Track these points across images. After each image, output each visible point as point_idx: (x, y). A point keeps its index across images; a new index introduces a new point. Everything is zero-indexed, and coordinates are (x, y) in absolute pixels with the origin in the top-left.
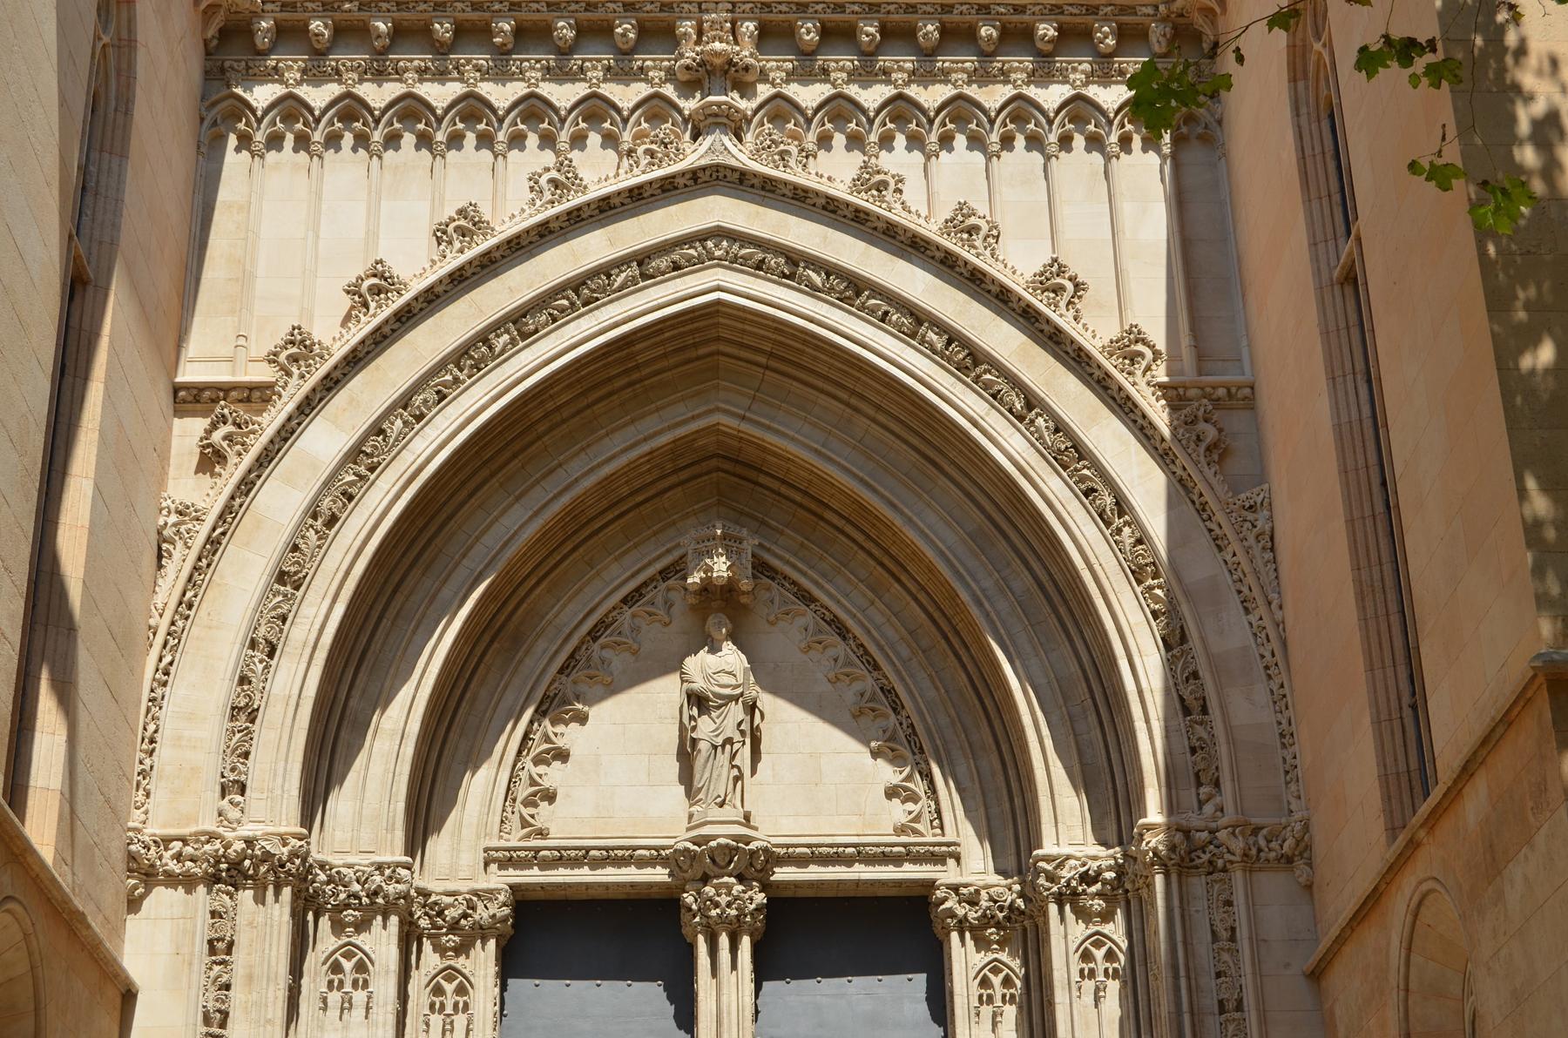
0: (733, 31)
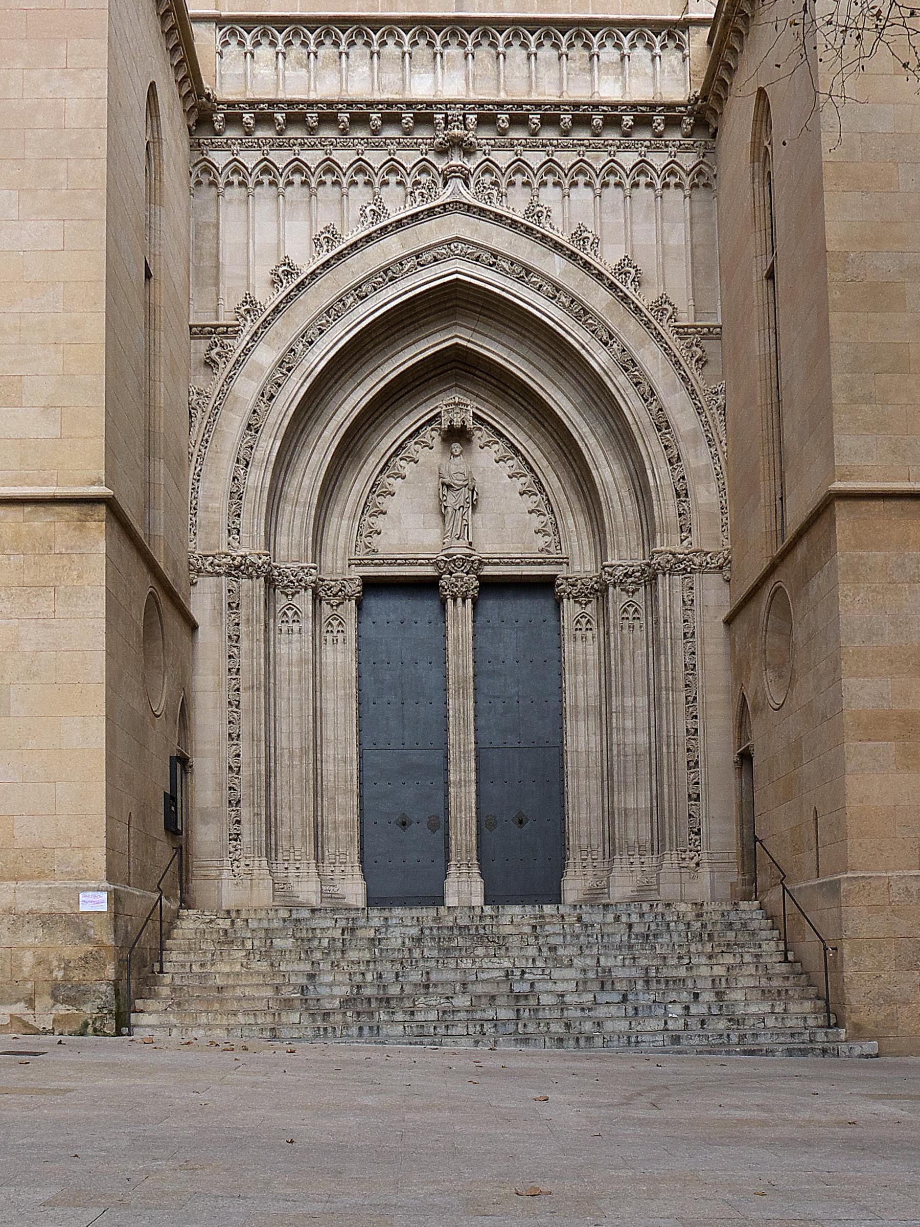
0: (465, 119)
